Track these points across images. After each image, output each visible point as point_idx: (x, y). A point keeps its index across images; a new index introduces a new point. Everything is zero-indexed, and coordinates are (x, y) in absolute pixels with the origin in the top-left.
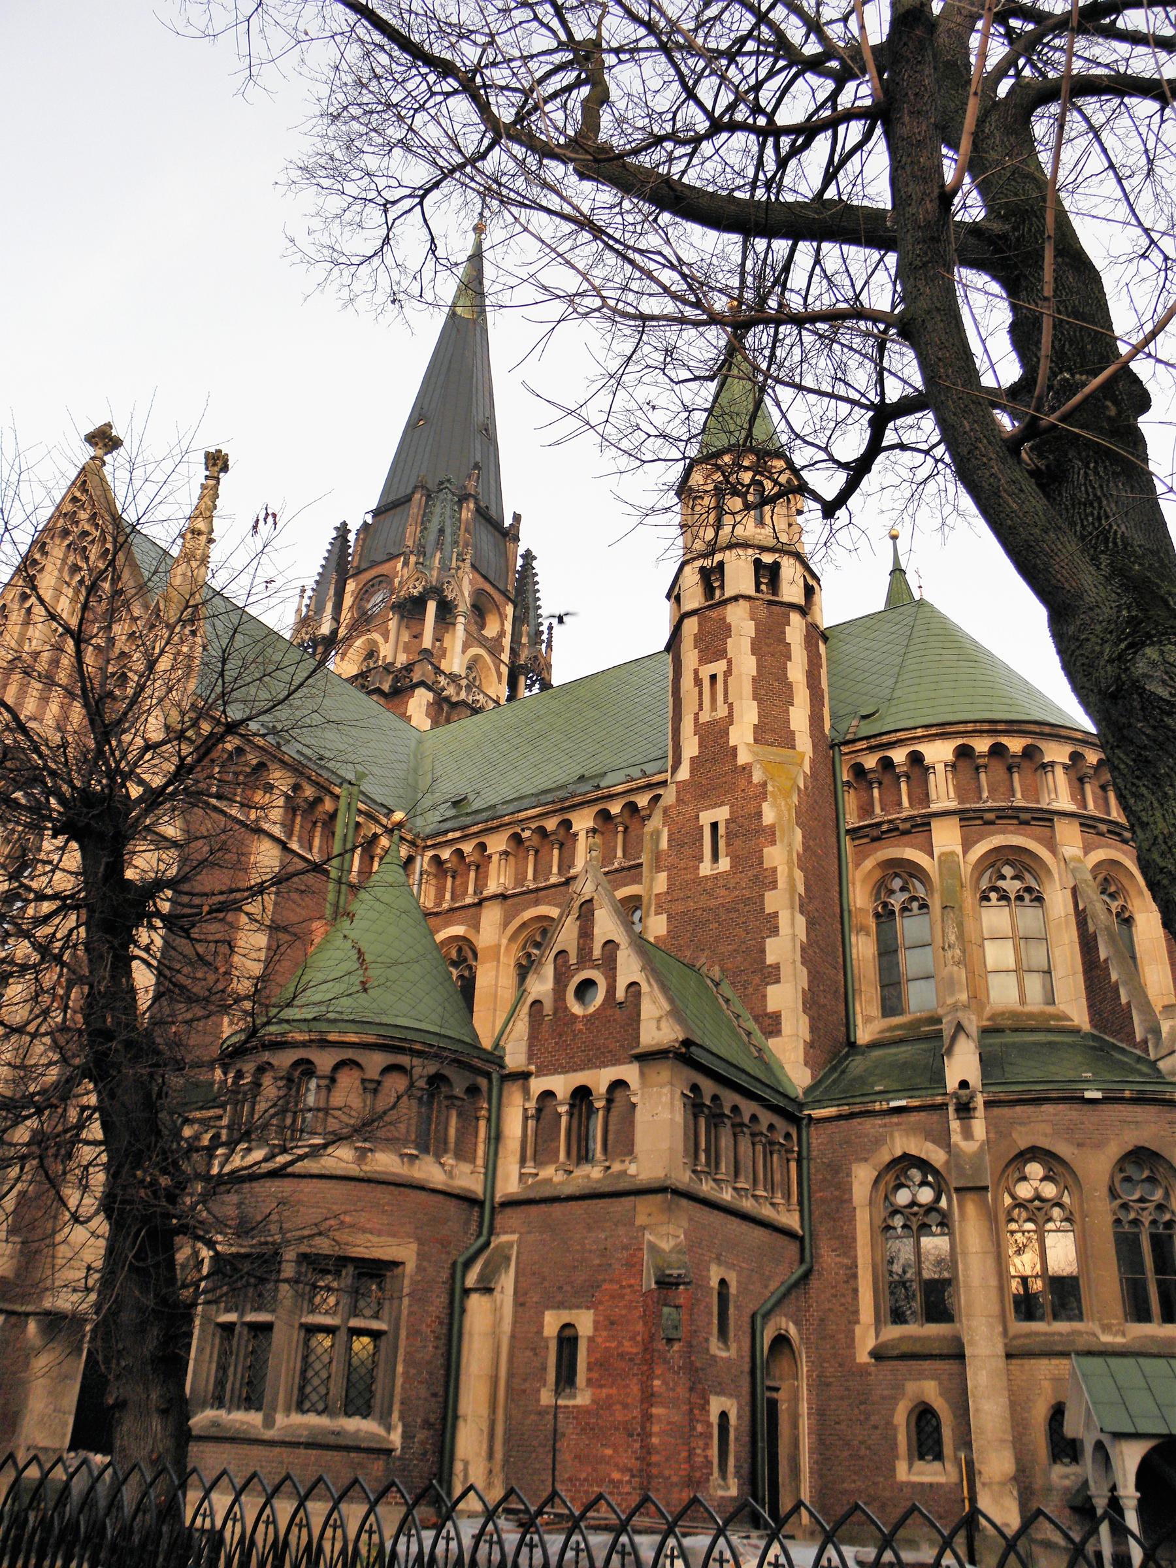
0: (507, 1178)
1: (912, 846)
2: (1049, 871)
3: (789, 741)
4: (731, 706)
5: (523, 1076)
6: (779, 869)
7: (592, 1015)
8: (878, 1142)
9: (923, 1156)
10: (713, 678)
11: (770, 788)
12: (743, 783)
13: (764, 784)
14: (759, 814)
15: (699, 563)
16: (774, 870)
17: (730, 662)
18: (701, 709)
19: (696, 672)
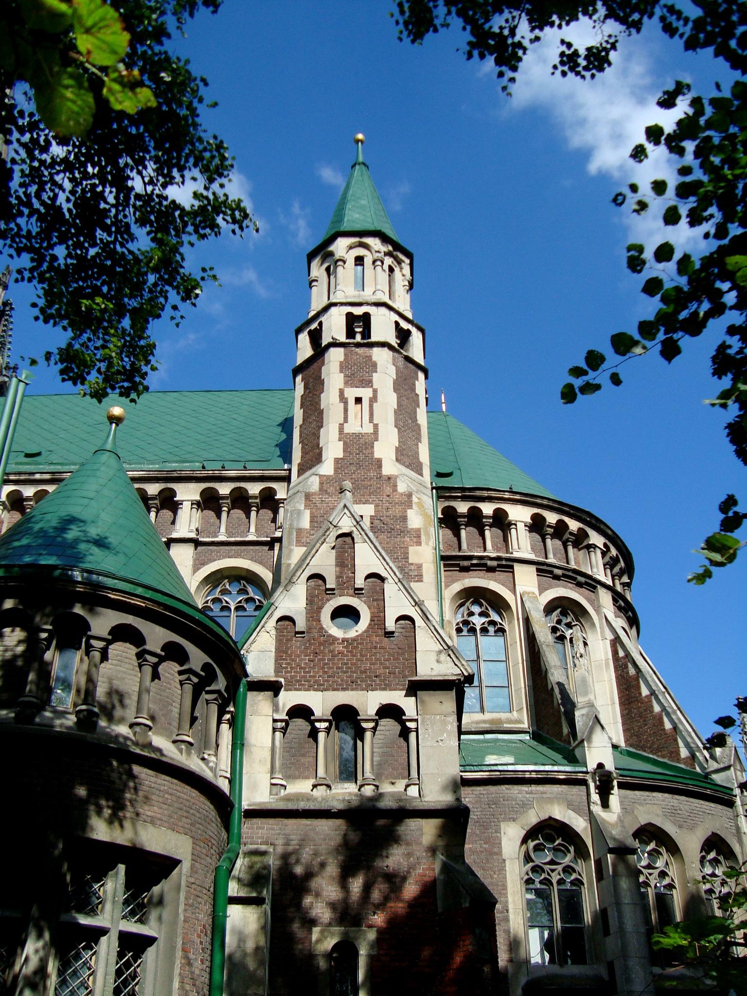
0: (254, 787)
1: (495, 581)
2: (593, 624)
3: (417, 468)
4: (376, 426)
5: (272, 688)
6: (424, 567)
7: (354, 640)
8: (525, 806)
9: (566, 821)
10: (358, 400)
11: (415, 499)
12: (388, 490)
13: (410, 495)
14: (404, 518)
15: (349, 309)
16: (420, 566)
17: (375, 391)
18: (346, 420)
19: (341, 392)
